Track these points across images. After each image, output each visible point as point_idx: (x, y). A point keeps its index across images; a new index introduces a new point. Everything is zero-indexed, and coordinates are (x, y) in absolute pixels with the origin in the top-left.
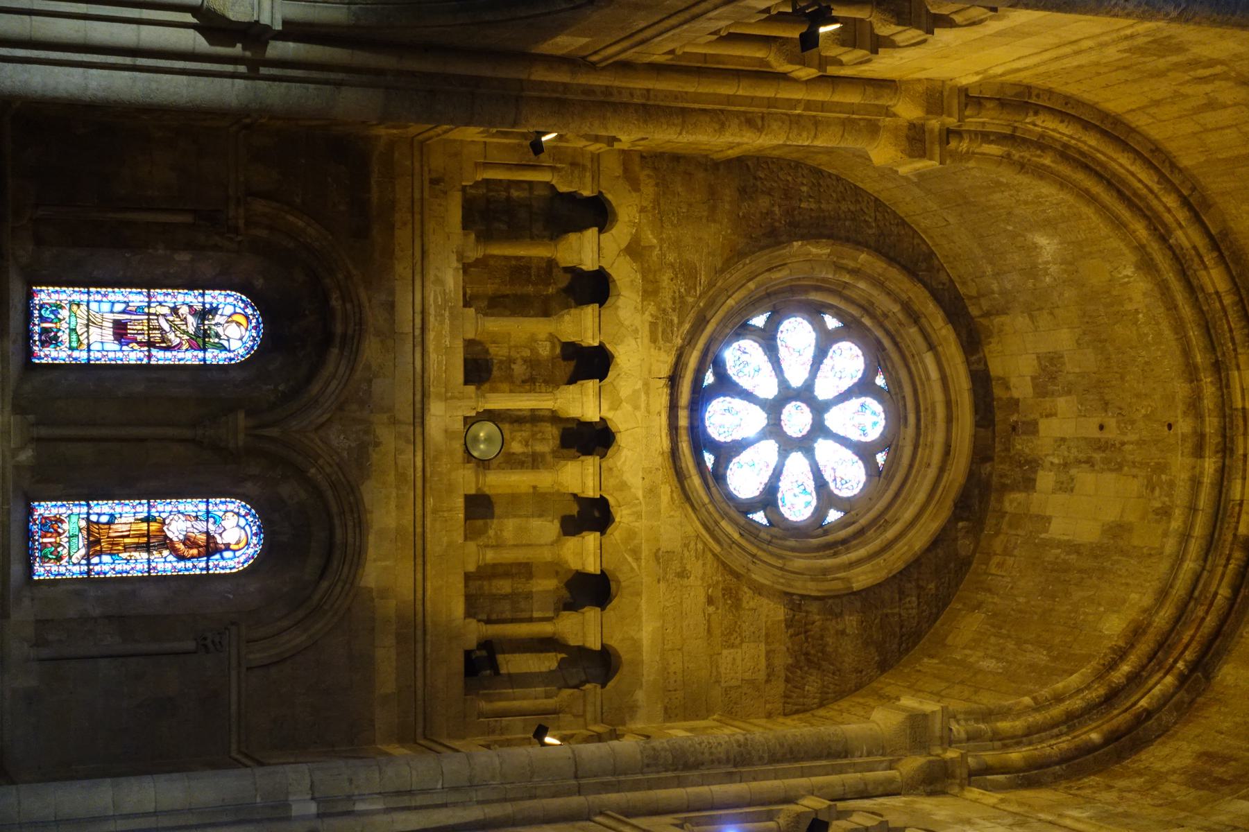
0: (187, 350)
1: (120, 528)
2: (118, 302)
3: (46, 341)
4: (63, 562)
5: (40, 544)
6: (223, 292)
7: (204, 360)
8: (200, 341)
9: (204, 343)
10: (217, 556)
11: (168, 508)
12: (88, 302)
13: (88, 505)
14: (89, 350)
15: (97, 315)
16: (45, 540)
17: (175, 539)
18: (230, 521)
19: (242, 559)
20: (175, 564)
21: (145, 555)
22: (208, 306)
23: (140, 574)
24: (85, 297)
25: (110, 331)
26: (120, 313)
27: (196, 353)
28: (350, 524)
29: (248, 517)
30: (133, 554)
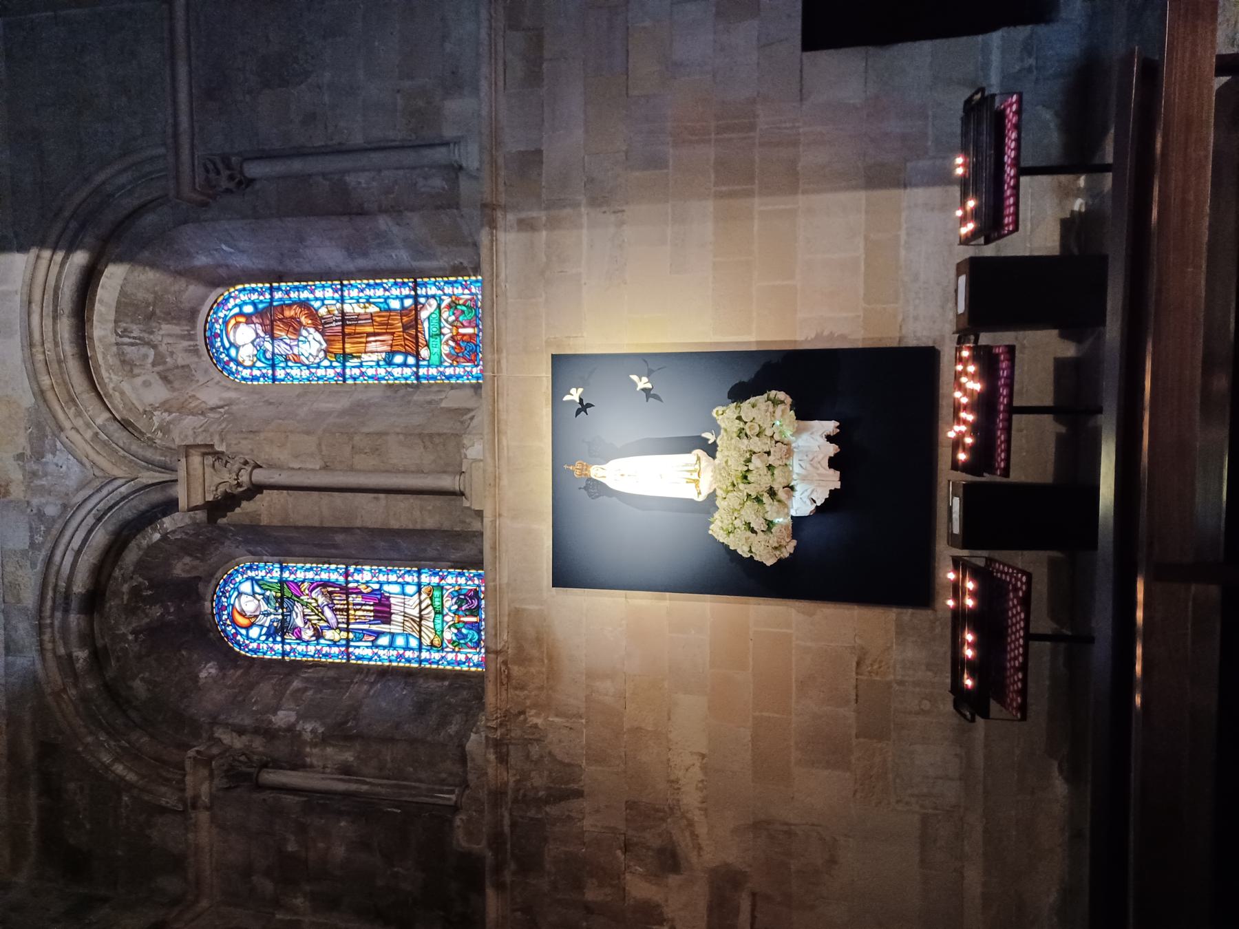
0: (303, 582)
1: (377, 348)
2: (384, 648)
3: (471, 598)
4: (447, 300)
5: (477, 326)
6: (260, 655)
7: (282, 569)
8: (287, 593)
9: (282, 590)
10: (261, 306)
11: (321, 372)
12: (420, 649)
13: (418, 378)
14: (419, 585)
15: (409, 630)
16: (470, 331)
17: (312, 330)
18: (246, 354)
19: (232, 303)
20: (311, 296)
21: (347, 308)
22: (279, 639)
23: (352, 282)
24: (425, 655)
25: (394, 609)
26: (383, 633)
27: (292, 578)
28: (49, 345)
29: (226, 359)
30: (362, 311)
